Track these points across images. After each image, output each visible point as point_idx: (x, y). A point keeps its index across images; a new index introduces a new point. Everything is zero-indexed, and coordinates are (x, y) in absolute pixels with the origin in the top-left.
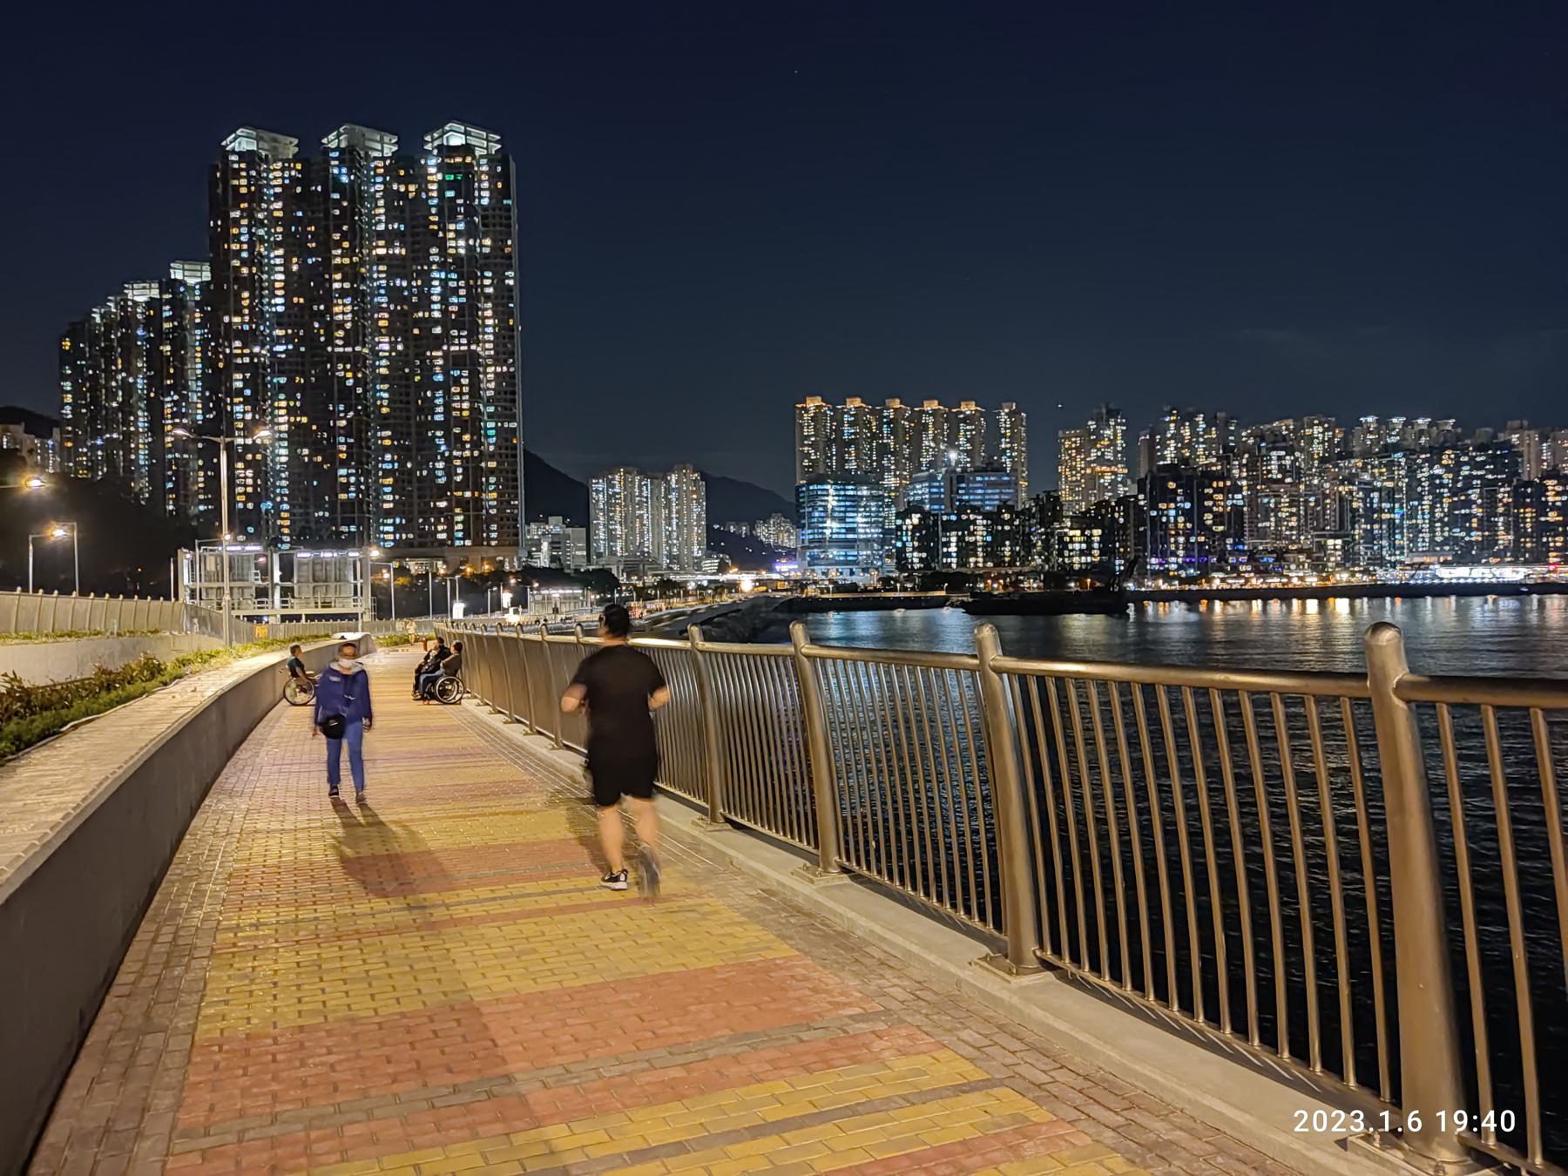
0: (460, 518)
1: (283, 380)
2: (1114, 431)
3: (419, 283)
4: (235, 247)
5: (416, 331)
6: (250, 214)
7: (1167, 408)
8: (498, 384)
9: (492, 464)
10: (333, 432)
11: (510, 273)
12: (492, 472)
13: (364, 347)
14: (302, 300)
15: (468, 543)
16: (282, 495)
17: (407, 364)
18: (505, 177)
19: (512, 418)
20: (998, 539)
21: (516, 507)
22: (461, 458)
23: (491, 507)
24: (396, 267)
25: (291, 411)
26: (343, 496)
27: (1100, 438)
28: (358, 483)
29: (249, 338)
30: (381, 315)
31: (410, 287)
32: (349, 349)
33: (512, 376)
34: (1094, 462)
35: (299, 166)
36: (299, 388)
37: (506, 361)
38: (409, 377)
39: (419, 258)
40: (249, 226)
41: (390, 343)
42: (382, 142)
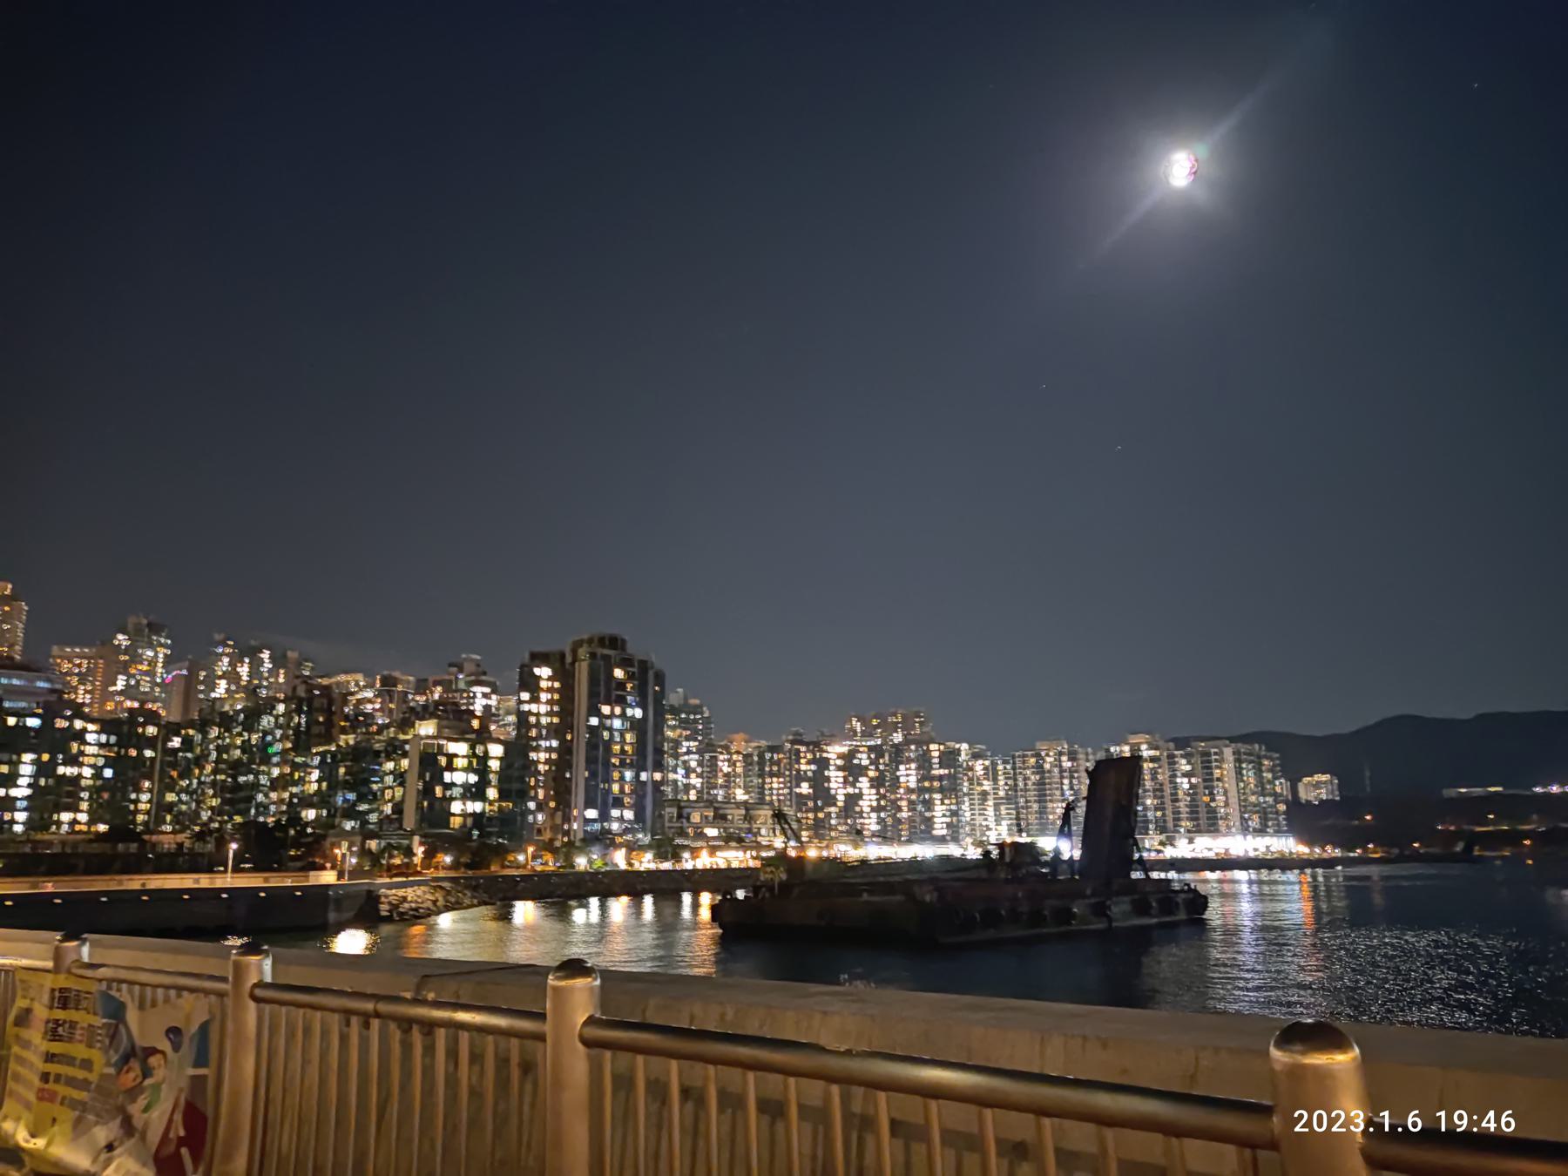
2: (156, 653)
7: (218, 637)
20: (128, 772)
27: (137, 659)
34: (121, 693)
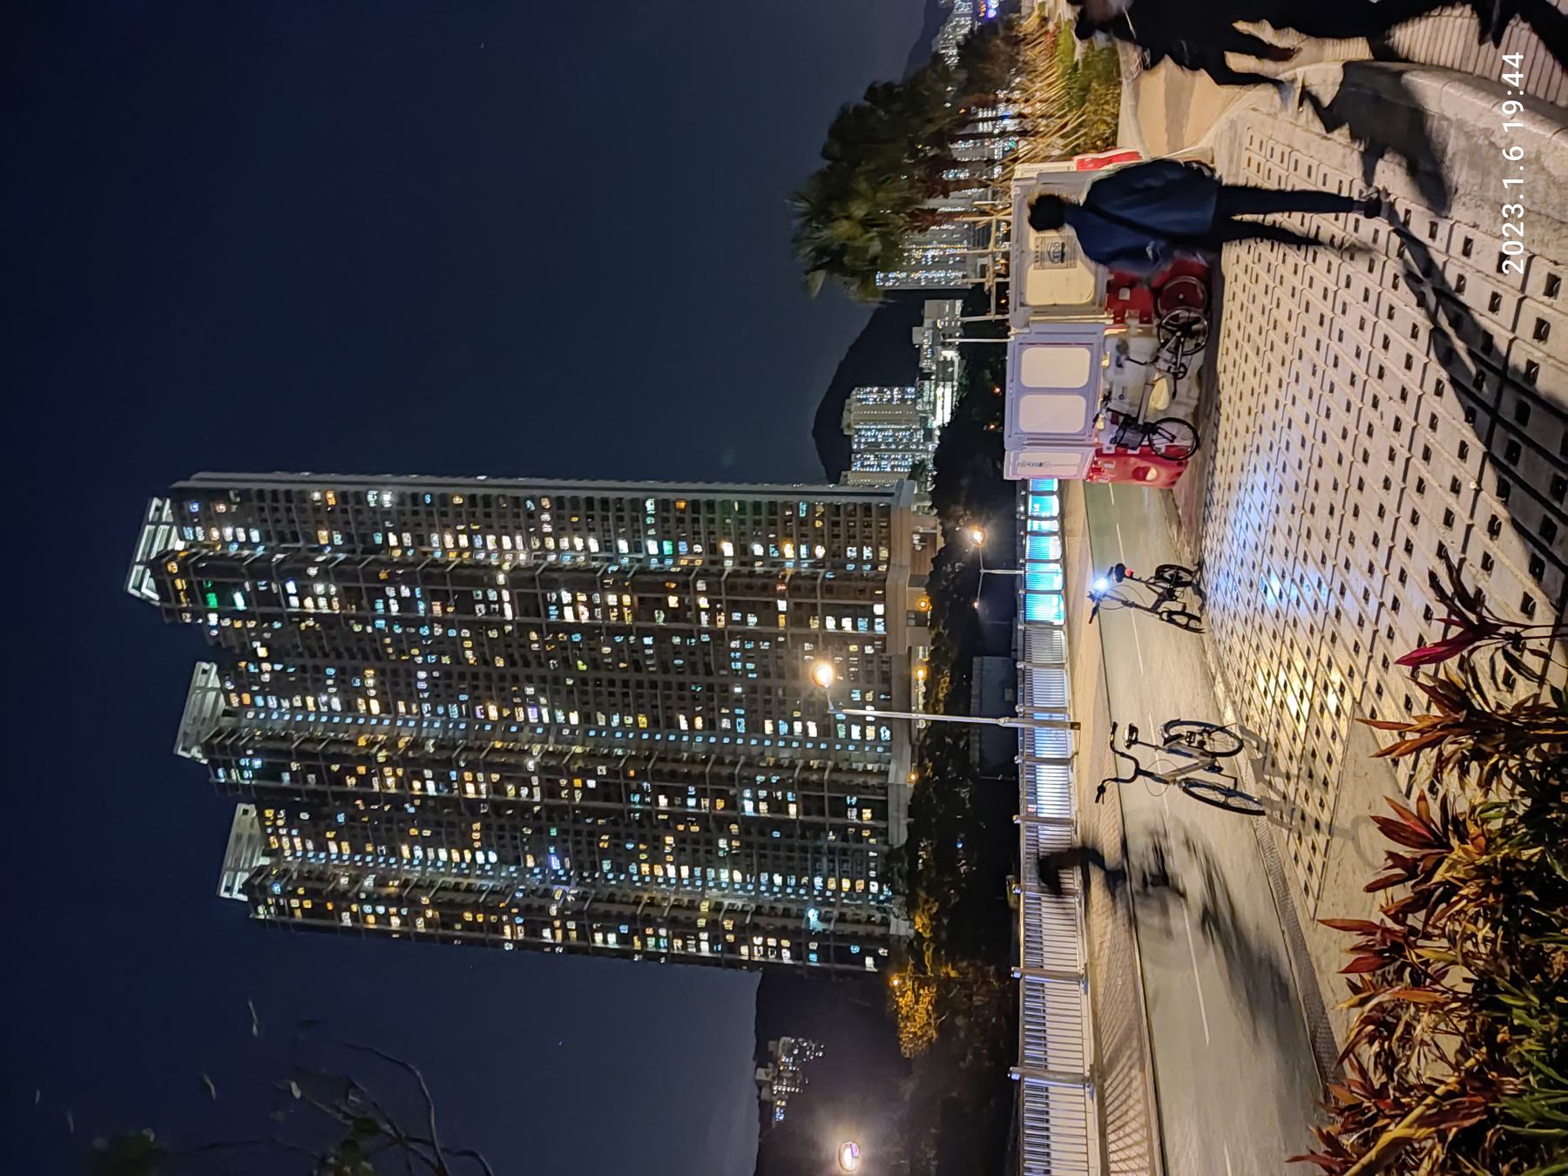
0: (830, 623)
1: (606, 865)
3: (415, 651)
4: (395, 922)
5: (500, 663)
6: (343, 899)
8: (576, 530)
9: (728, 548)
10: (677, 816)
11: (371, 498)
12: (742, 551)
13: (528, 753)
14: (477, 826)
15: (879, 609)
16: (798, 885)
17: (558, 680)
18: (210, 496)
19: (638, 506)
21: (811, 508)
22: (713, 612)
23: (811, 554)
24: (396, 685)
25: (656, 858)
26: (793, 809)
28: (766, 785)
29: (536, 919)
30: (479, 715)
31: (425, 666)
32: (535, 780)
33: (559, 503)
35: (269, 813)
36: (616, 844)
37: (531, 515)
38: (582, 680)
39: (376, 651)
40: (361, 902)
41: (524, 705)
42: (205, 690)
